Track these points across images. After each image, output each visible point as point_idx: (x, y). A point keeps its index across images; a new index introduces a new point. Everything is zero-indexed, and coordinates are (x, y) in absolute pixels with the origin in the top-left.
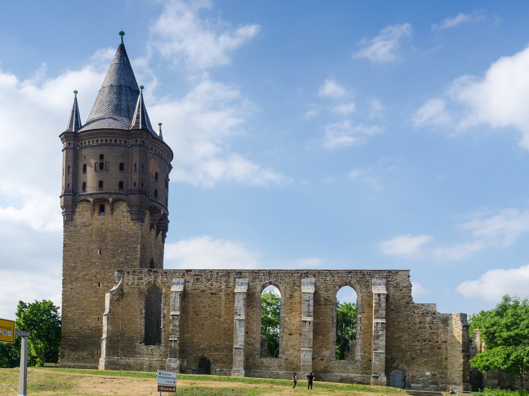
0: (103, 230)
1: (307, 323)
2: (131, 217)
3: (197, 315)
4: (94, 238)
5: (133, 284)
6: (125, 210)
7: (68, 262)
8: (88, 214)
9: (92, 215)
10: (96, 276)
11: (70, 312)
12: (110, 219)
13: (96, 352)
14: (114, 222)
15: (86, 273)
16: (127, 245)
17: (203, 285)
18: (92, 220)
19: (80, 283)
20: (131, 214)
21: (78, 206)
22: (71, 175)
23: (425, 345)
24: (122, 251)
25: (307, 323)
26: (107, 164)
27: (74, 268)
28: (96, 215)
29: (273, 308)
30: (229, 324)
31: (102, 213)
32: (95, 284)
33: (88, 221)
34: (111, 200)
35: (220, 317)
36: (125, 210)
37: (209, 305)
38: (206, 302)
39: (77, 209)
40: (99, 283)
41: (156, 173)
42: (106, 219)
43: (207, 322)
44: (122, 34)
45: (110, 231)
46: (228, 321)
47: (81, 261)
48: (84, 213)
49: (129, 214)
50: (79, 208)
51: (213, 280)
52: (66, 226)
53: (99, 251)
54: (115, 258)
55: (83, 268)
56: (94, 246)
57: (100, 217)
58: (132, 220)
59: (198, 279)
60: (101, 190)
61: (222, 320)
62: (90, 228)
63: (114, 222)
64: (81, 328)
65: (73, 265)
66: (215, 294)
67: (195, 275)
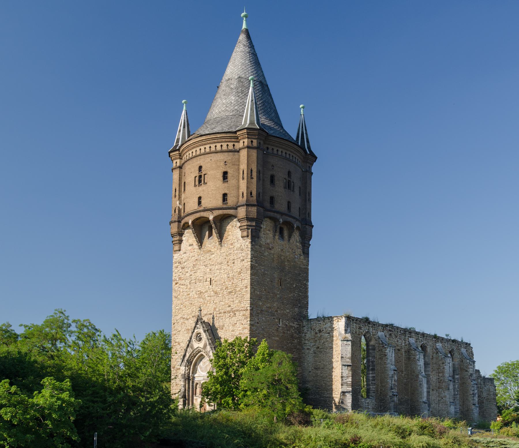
0: (282, 258)
9: (274, 236)
10: (277, 311)
15: (268, 305)
19: (265, 317)
22: (255, 180)
23: (58, 394)
29: (267, 354)
32: (277, 320)
48: (268, 232)
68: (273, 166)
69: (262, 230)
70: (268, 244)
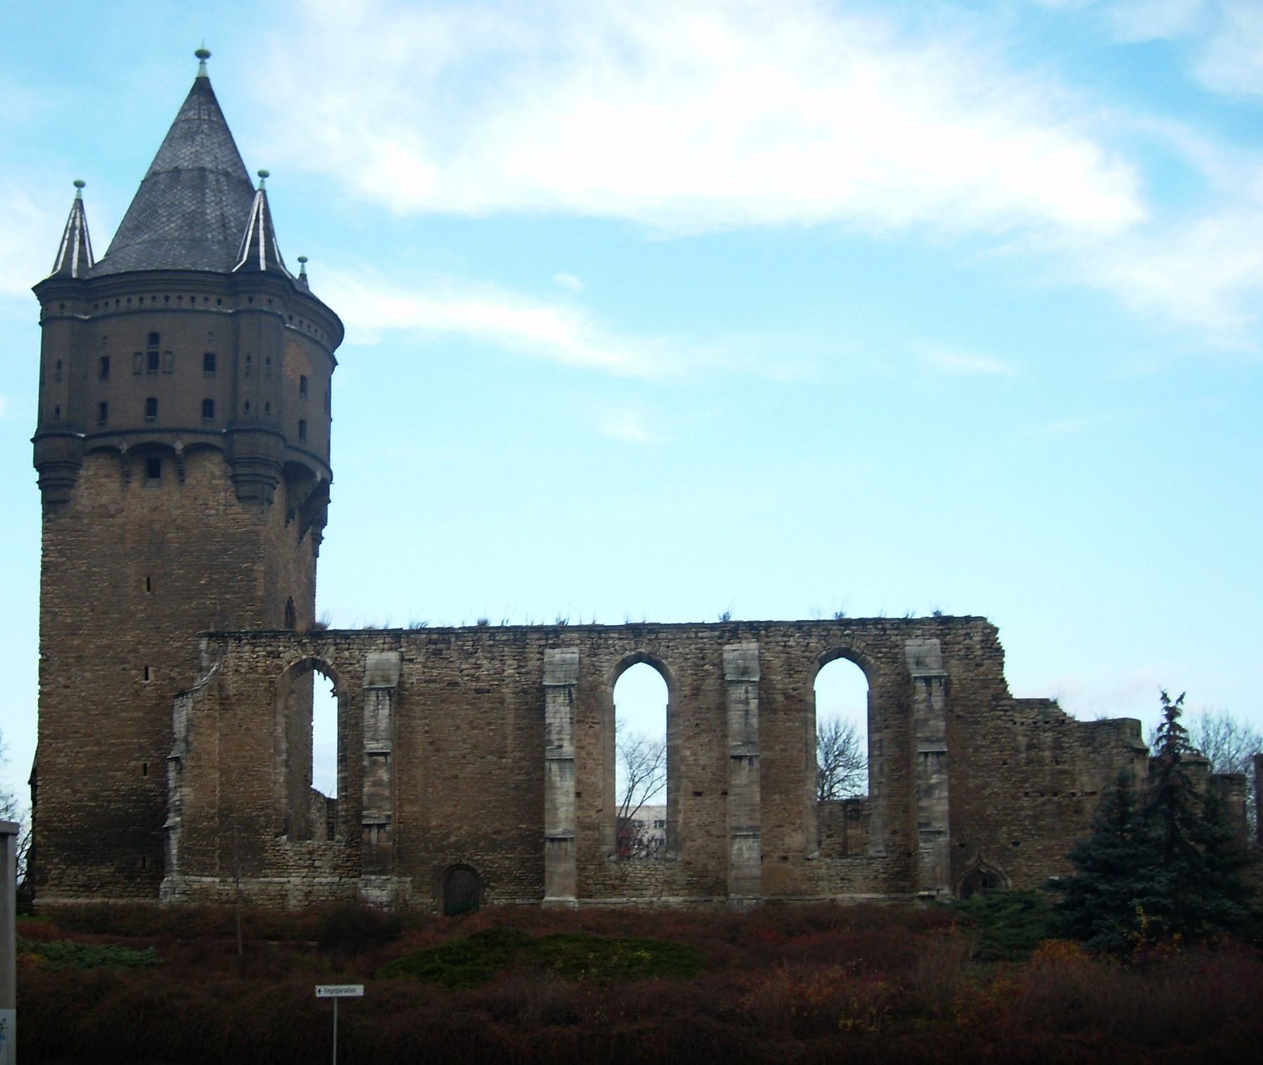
0: (157, 526)
1: (745, 763)
2: (237, 491)
3: (438, 750)
5: (252, 669)
6: (218, 473)
7: (55, 614)
8: (113, 485)
10: (136, 651)
11: (61, 750)
13: (140, 863)
14: (187, 502)
15: (105, 642)
17: (456, 667)
18: (123, 499)
20: (236, 483)
21: (85, 464)
25: (745, 763)
26: (168, 357)
27: (74, 630)
28: (135, 485)
30: (528, 774)
31: (152, 482)
34: (179, 446)
35: (502, 754)
36: (218, 473)
37: (471, 723)
38: (463, 713)
39: (82, 472)
40: (146, 669)
41: (303, 378)
43: (470, 768)
44: (203, 55)
46: (525, 763)
48: (103, 480)
49: (229, 482)
50: (87, 469)
51: (480, 654)
52: (51, 516)
58: (239, 498)
59: (438, 653)
60: (152, 420)
61: (508, 761)
62: (119, 520)
63: (187, 502)
64: (95, 797)
65: (69, 620)
66: (488, 691)
67: (430, 642)
68: (105, 338)
69: (82, 480)
70: (101, 506)
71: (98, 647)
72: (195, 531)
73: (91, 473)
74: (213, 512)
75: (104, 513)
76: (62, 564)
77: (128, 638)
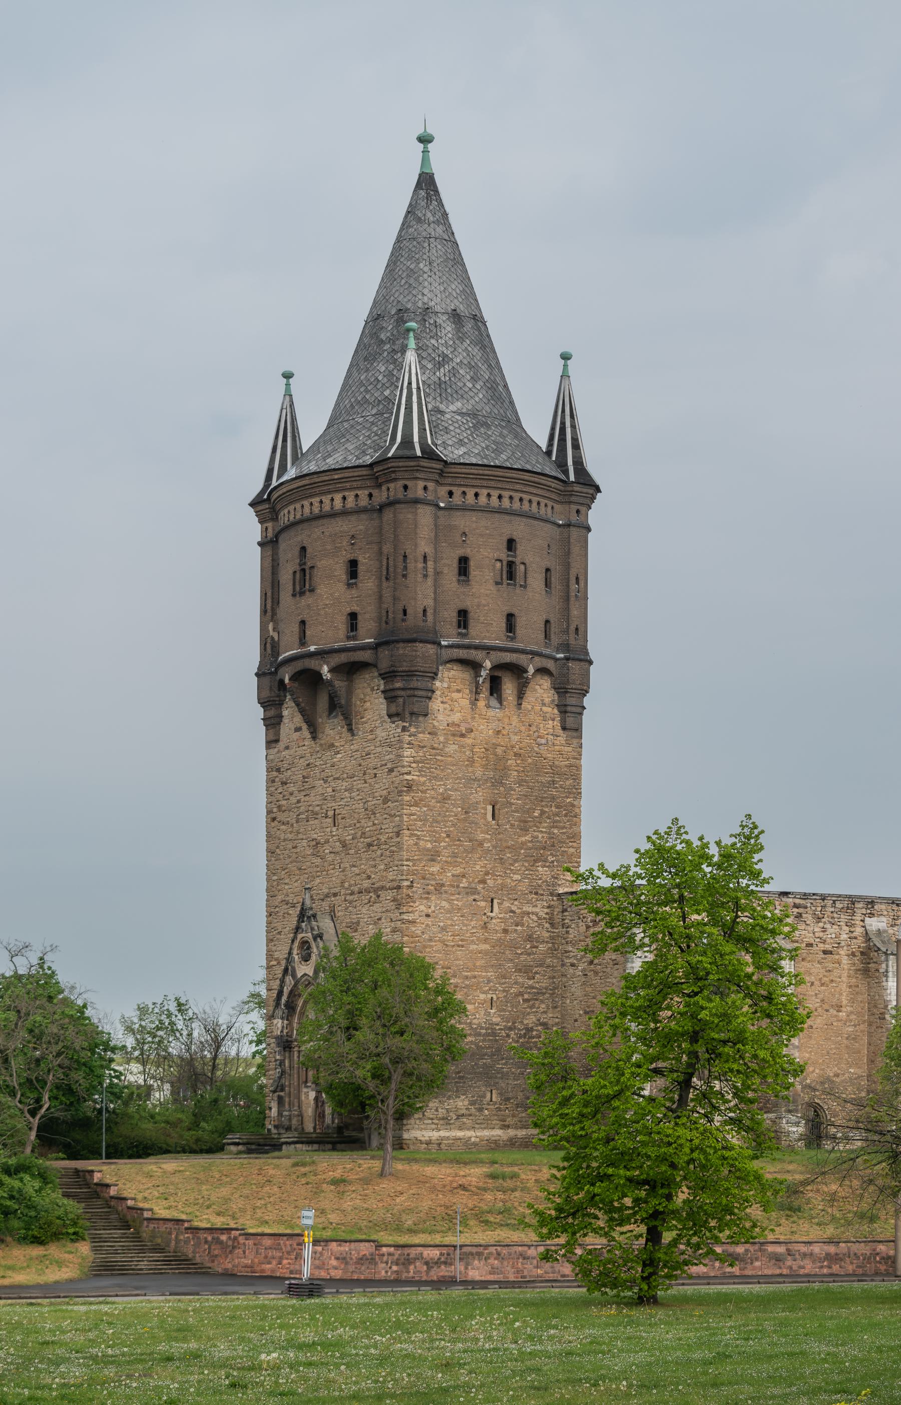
0: (499, 751)
4: (479, 773)
12: (515, 720)
14: (523, 728)
16: (553, 798)
21: (440, 675)
24: (543, 813)
28: (481, 704)
33: (464, 721)
42: (506, 720)
45: (516, 755)
47: (448, 836)
48: (456, 695)
53: (490, 808)
54: (525, 830)
55: (455, 855)
56: (479, 795)
57: (491, 713)
58: (564, 729)
62: (468, 741)
63: (523, 728)
65: (429, 845)
69: (438, 693)
71: (453, 876)
72: (530, 760)
73: (445, 685)
74: (543, 741)
75: (459, 733)
76: (424, 783)
77: (478, 867)
